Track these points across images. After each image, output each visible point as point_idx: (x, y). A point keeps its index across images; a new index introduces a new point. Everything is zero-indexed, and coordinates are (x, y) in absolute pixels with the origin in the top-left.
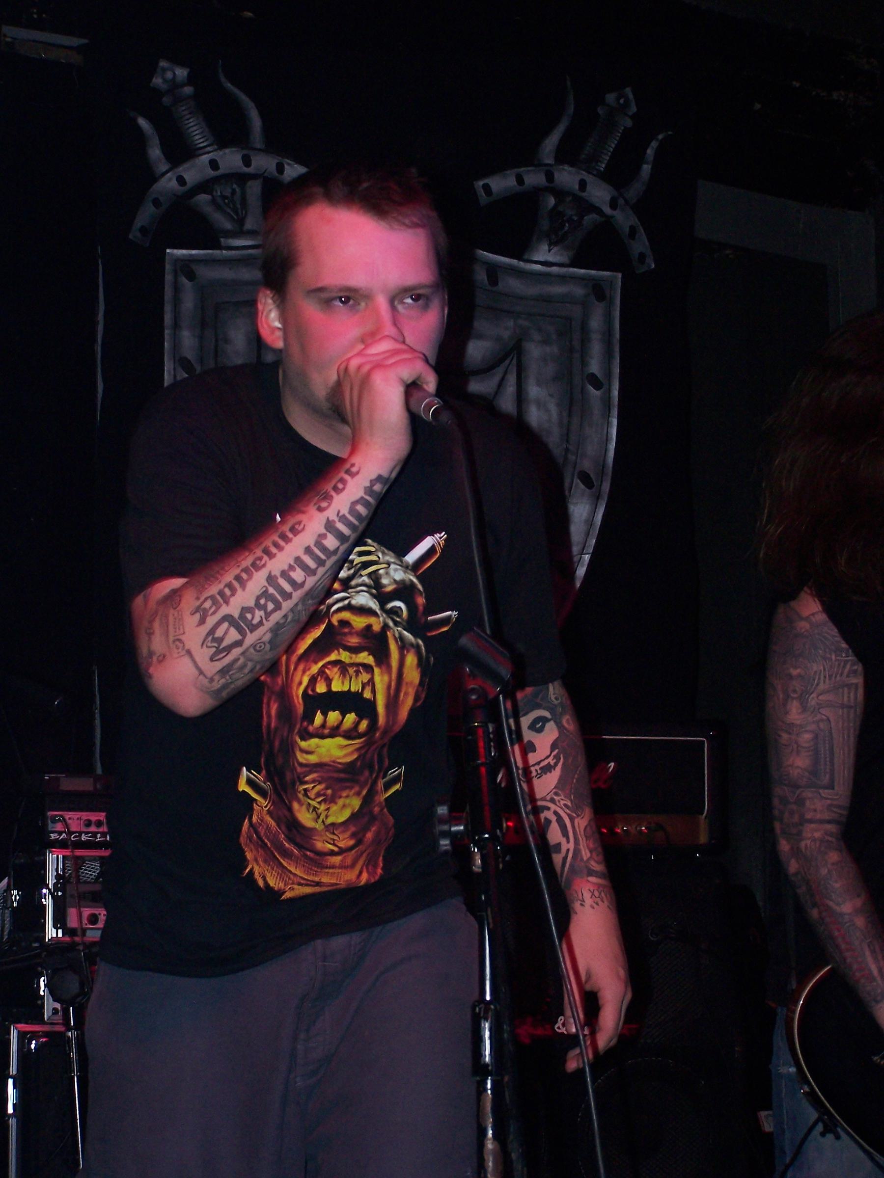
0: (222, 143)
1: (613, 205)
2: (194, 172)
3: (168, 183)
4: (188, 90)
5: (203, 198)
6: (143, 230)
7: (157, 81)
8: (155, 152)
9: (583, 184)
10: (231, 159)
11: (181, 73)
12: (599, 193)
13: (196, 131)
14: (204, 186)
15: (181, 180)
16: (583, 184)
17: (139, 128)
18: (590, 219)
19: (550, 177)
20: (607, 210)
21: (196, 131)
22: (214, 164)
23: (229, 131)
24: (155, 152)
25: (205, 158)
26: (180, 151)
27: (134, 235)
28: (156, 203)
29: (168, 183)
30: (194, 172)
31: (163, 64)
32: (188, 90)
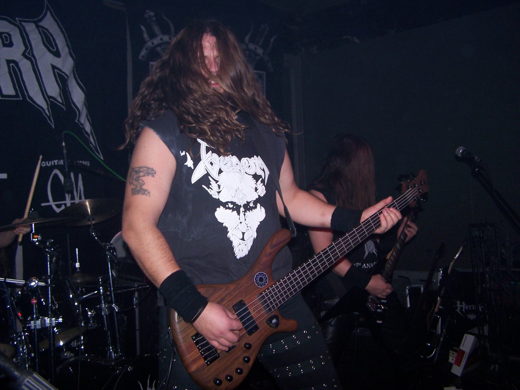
0: (164, 33)
1: (263, 54)
2: (156, 41)
3: (149, 44)
4: (154, 19)
5: (159, 49)
6: (143, 56)
7: (146, 16)
8: (146, 35)
9: (256, 49)
10: (166, 38)
11: (152, 14)
12: (260, 51)
13: (156, 29)
14: (159, 45)
15: (153, 43)
16: (256, 49)
17: (141, 29)
18: (258, 57)
19: (247, 46)
20: (262, 56)
21: (156, 29)
22: (161, 39)
23: (165, 31)
24: (146, 35)
25: (159, 38)
26: (152, 36)
27: (140, 57)
28: (146, 49)
29: (149, 44)
30: (156, 41)
31: (147, 11)
32: (154, 19)
